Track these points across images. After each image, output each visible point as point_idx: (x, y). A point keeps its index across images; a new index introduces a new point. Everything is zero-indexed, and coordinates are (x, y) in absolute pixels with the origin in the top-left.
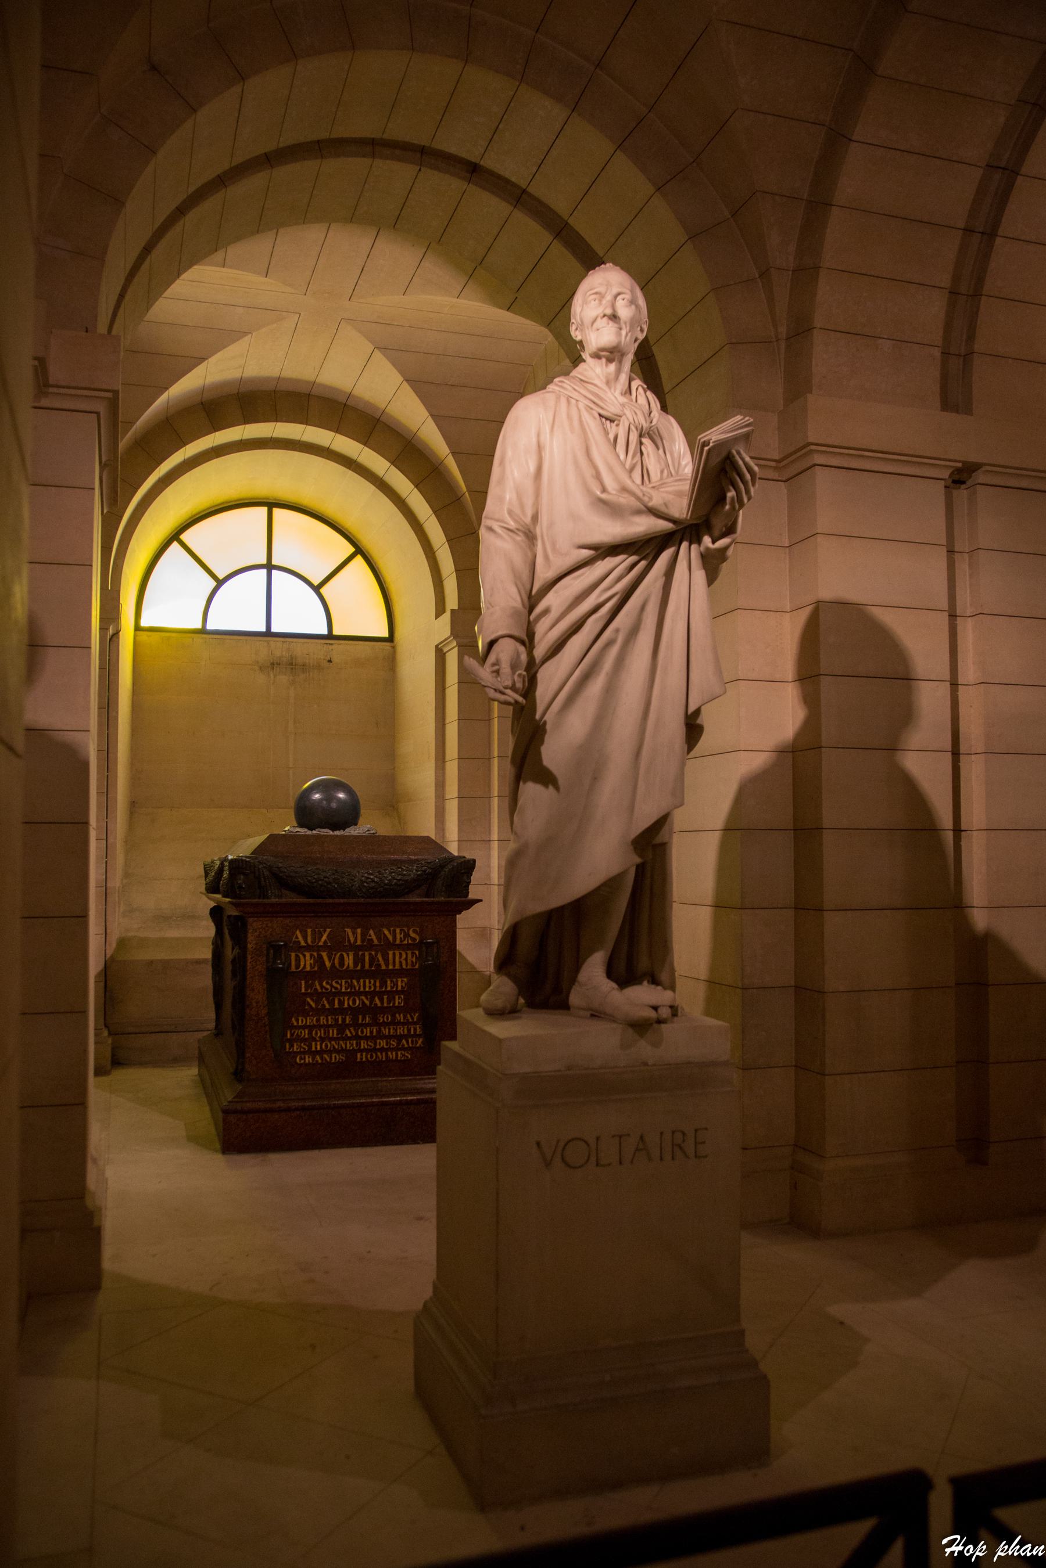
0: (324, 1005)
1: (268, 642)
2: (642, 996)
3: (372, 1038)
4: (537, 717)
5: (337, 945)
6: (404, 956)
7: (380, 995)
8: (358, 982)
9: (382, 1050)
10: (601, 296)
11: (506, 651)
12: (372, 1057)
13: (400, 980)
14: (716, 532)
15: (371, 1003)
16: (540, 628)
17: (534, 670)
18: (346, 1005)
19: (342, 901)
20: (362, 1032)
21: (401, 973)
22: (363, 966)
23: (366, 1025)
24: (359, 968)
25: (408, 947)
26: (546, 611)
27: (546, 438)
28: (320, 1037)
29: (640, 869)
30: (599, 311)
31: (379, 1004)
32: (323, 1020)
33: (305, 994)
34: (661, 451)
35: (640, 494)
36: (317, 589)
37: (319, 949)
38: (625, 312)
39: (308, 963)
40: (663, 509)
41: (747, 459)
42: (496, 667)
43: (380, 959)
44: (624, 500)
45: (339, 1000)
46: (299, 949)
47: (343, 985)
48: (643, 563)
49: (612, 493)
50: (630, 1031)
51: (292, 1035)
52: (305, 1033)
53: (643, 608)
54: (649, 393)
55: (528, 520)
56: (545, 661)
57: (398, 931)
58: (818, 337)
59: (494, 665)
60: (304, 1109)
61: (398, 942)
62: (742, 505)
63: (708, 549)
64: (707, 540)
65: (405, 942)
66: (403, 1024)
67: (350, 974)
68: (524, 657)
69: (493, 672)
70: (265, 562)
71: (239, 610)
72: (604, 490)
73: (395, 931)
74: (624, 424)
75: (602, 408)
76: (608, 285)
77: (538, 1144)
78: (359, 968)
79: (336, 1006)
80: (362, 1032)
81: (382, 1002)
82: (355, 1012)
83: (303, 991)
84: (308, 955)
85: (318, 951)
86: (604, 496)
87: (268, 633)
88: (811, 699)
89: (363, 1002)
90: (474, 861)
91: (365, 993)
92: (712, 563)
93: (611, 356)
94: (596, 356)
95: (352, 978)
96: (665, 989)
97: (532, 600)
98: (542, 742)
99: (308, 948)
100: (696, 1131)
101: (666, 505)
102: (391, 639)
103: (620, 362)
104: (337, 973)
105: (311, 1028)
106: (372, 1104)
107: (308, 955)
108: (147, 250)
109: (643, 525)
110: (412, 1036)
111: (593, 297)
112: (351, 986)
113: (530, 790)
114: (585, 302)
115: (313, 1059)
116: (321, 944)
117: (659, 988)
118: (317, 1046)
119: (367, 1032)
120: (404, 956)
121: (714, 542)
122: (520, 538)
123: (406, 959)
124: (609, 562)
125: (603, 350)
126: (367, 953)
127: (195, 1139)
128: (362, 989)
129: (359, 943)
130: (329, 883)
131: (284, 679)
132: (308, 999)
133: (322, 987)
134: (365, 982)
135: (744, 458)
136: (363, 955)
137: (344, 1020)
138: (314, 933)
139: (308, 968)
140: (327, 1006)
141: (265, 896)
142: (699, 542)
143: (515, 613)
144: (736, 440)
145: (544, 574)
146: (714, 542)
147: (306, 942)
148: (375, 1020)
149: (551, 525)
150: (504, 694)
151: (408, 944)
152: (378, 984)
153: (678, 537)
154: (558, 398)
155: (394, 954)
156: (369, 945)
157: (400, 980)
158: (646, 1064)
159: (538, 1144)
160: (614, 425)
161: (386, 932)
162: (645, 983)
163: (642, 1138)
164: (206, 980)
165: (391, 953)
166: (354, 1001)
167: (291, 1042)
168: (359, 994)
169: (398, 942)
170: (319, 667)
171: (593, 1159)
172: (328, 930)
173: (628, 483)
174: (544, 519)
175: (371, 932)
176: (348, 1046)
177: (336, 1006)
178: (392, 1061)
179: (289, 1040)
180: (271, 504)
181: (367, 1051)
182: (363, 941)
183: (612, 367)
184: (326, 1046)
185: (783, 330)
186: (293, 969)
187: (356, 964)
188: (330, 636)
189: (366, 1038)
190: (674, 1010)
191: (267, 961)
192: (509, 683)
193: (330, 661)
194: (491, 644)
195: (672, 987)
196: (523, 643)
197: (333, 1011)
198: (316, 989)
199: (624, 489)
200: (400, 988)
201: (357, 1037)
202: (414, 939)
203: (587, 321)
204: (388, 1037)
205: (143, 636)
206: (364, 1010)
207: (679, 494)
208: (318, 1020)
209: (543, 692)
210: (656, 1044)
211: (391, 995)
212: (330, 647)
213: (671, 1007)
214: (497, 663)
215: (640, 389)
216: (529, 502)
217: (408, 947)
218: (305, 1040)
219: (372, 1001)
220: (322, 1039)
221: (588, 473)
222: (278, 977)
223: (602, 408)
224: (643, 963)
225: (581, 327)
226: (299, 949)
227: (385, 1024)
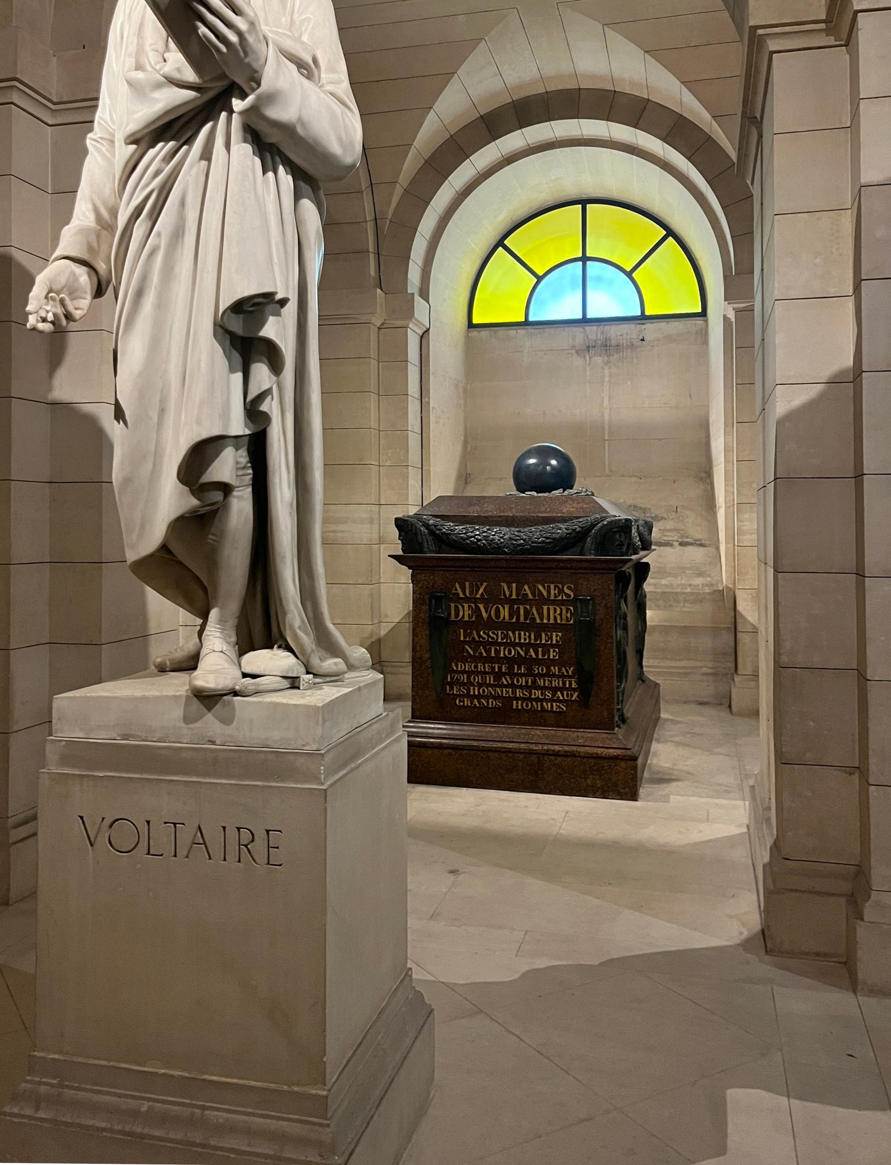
0: (481, 653)
3: (527, 687)
7: (535, 647)
8: (514, 634)
9: (537, 700)
12: (527, 706)
13: (554, 634)
15: (526, 654)
18: (502, 655)
20: (518, 681)
21: (556, 627)
24: (514, 620)
25: (562, 603)
28: (478, 682)
31: (534, 656)
37: (476, 601)
43: (535, 612)
45: (496, 649)
46: (458, 600)
48: (185, 148)
51: (452, 678)
53: (182, 203)
57: (552, 586)
61: (552, 597)
64: (238, 105)
65: (560, 598)
66: (558, 676)
67: (505, 626)
73: (549, 587)
78: (514, 620)
79: (493, 654)
80: (518, 681)
81: (536, 653)
82: (511, 661)
83: (462, 639)
84: (466, 606)
85: (475, 603)
89: (518, 653)
91: (521, 645)
99: (466, 599)
104: (493, 624)
105: (469, 673)
107: (466, 606)
110: (567, 689)
112: (506, 636)
115: (471, 703)
116: (478, 596)
119: (523, 681)
123: (561, 614)
126: (521, 607)
128: (517, 641)
130: (479, 540)
132: (467, 647)
133: (479, 636)
134: (520, 635)
137: (500, 668)
138: (471, 586)
139: (466, 618)
140: (485, 655)
141: (421, 552)
147: (464, 594)
151: (562, 600)
152: (532, 637)
155: (548, 609)
156: (523, 600)
157: (554, 634)
161: (541, 588)
165: (545, 608)
166: (510, 653)
167: (451, 684)
168: (514, 645)
169: (552, 597)
172: (485, 584)
175: (526, 587)
176: (506, 692)
177: (493, 654)
178: (547, 711)
179: (450, 684)
181: (523, 699)
182: (518, 595)
184: (484, 691)
186: (453, 618)
187: (511, 617)
189: (521, 687)
197: (489, 660)
198: (474, 638)
200: (554, 642)
201: (512, 686)
202: (568, 595)
204: (545, 688)
206: (519, 660)
208: (476, 667)
211: (546, 648)
218: (464, 684)
219: (527, 652)
220: (480, 685)
226: (458, 600)
227: (541, 676)
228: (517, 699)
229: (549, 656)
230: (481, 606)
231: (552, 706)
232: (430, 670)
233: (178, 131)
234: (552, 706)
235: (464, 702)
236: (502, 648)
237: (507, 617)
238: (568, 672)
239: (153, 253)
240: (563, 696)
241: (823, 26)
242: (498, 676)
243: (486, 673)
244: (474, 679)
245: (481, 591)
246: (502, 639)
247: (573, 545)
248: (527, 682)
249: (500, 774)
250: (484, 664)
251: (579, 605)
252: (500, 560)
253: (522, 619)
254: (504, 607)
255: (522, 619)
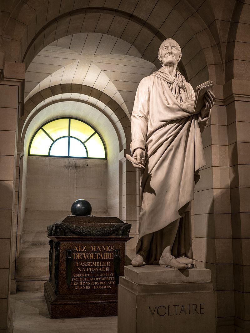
0: (84, 270)
1: (68, 159)
2: (183, 261)
3: (99, 281)
4: (149, 173)
5: (88, 251)
6: (109, 255)
7: (101, 267)
8: (95, 263)
9: (102, 285)
10: (167, 47)
11: (138, 152)
12: (98, 287)
14: (203, 116)
15: (98, 270)
16: (149, 146)
17: (148, 159)
19: (90, 237)
21: (108, 260)
22: (96, 258)
23: (97, 277)
25: (110, 252)
26: (151, 141)
27: (151, 89)
29: (181, 219)
30: (167, 52)
32: (83, 275)
33: (78, 267)
34: (186, 92)
35: (179, 105)
36: (83, 143)
37: (82, 252)
38: (175, 52)
39: (79, 257)
40: (187, 109)
41: (212, 93)
42: (136, 157)
43: (101, 255)
44: (174, 107)
47: (89, 264)
49: (171, 105)
50: (179, 271)
51: (73, 280)
52: (77, 279)
53: (181, 139)
54: (182, 76)
55: (146, 114)
56: (151, 155)
57: (107, 247)
58: (235, 62)
59: (135, 156)
60: (76, 304)
61: (107, 250)
62: (210, 107)
63: (200, 121)
64: (200, 118)
65: (109, 250)
66: (108, 277)
67: (92, 261)
68: (144, 154)
69: (135, 159)
70: (68, 135)
71: (60, 150)
72: (168, 104)
74: (175, 84)
75: (168, 80)
76: (170, 43)
77: (149, 307)
79: (88, 271)
81: (102, 270)
82: (93, 273)
86: (168, 106)
87: (68, 157)
88: (236, 171)
90: (131, 225)
91: (97, 267)
92: (202, 126)
93: (171, 65)
94: (166, 65)
95: (92, 262)
96: (190, 259)
97: (147, 138)
98: (150, 180)
99: (79, 252)
100: (201, 304)
101: (187, 108)
102: (106, 159)
103: (173, 67)
104: (87, 260)
105: (79, 278)
106: (98, 303)
107: (79, 254)
108: (34, 40)
109: (180, 114)
111: (165, 47)
112: (92, 264)
113: (147, 195)
114: (163, 49)
115: (80, 288)
117: (188, 258)
118: (81, 284)
119: (97, 279)
120: (109, 255)
121: (202, 120)
122: (143, 119)
123: (110, 256)
124: (170, 126)
125: (168, 63)
127: (42, 314)
129: (95, 250)
130: (86, 231)
131: (73, 171)
133: (83, 264)
134: (96, 263)
135: (211, 93)
136: (96, 254)
137: (90, 275)
138: (81, 247)
140: (85, 271)
141: (65, 235)
142: (198, 119)
143: (142, 141)
144: (208, 87)
145: (150, 129)
146: (202, 120)
148: (99, 275)
149: (153, 115)
150: (138, 165)
152: (101, 264)
153: (191, 118)
154: (155, 78)
155: (106, 254)
156: (98, 251)
158: (184, 282)
159: (149, 307)
160: (171, 85)
161: (103, 247)
162: (183, 256)
163: (183, 306)
164: (47, 264)
167: (73, 282)
169: (107, 250)
170: (84, 167)
171: (167, 313)
173: (176, 101)
174: (150, 113)
175: (99, 247)
176: (91, 283)
177: (88, 271)
178: (105, 289)
180: (70, 118)
181: (97, 285)
183: (171, 68)
184: (84, 284)
185: (224, 61)
186: (74, 259)
187: (94, 257)
188: (87, 158)
189: (97, 281)
190: (193, 266)
191: (66, 256)
192: (139, 162)
193: (87, 165)
194: (135, 150)
195: (192, 258)
196: (144, 150)
197: (86, 272)
199: (175, 104)
201: (94, 281)
202: (112, 249)
203: (163, 55)
204: (104, 281)
205: (31, 157)
206: (96, 272)
207: (191, 105)
208: (82, 275)
209: (150, 165)
210: (187, 275)
211: (105, 267)
212: (88, 161)
213: (192, 264)
214: (136, 156)
215: (179, 74)
216: (146, 108)
217: (110, 252)
218: (77, 282)
219: (99, 269)
220: (83, 282)
221: (164, 99)
222: (69, 262)
223: (168, 80)
224: (183, 250)
225: (161, 57)
226: (76, 252)
227: (103, 277)
228: (95, 285)
229: (106, 270)
230: (84, 254)
231: (106, 287)
232: (66, 278)
233: (179, 121)
234: (106, 287)
235: (77, 288)
236: (91, 268)
237: (92, 258)
238: (111, 275)
239: (171, 150)
240: (110, 283)
241: (222, 101)
242: (89, 278)
243: (85, 277)
244: (81, 280)
245: (84, 249)
246: (91, 265)
247: (113, 233)
248: (98, 279)
249: (92, 311)
250: (84, 274)
251: (115, 253)
252: (91, 238)
253: (97, 258)
254: (91, 254)
255: (97, 258)
